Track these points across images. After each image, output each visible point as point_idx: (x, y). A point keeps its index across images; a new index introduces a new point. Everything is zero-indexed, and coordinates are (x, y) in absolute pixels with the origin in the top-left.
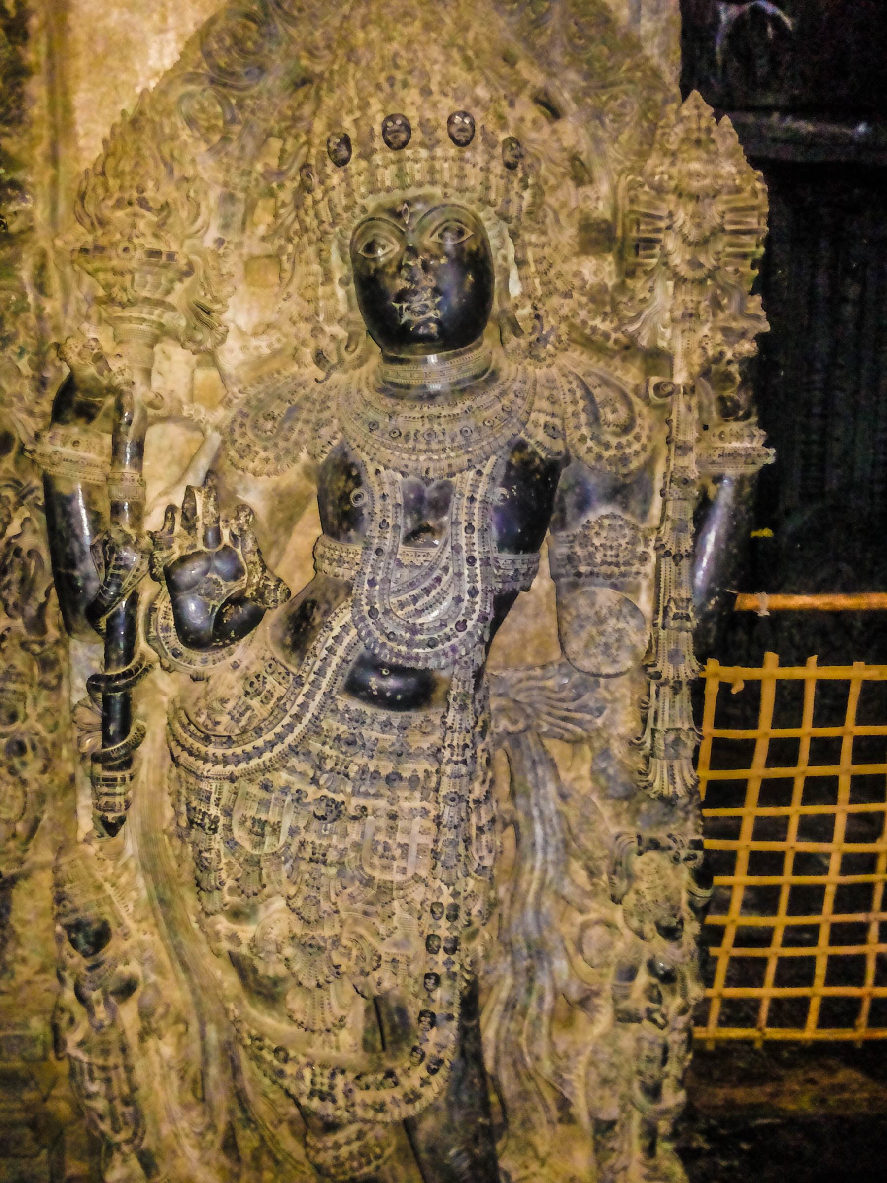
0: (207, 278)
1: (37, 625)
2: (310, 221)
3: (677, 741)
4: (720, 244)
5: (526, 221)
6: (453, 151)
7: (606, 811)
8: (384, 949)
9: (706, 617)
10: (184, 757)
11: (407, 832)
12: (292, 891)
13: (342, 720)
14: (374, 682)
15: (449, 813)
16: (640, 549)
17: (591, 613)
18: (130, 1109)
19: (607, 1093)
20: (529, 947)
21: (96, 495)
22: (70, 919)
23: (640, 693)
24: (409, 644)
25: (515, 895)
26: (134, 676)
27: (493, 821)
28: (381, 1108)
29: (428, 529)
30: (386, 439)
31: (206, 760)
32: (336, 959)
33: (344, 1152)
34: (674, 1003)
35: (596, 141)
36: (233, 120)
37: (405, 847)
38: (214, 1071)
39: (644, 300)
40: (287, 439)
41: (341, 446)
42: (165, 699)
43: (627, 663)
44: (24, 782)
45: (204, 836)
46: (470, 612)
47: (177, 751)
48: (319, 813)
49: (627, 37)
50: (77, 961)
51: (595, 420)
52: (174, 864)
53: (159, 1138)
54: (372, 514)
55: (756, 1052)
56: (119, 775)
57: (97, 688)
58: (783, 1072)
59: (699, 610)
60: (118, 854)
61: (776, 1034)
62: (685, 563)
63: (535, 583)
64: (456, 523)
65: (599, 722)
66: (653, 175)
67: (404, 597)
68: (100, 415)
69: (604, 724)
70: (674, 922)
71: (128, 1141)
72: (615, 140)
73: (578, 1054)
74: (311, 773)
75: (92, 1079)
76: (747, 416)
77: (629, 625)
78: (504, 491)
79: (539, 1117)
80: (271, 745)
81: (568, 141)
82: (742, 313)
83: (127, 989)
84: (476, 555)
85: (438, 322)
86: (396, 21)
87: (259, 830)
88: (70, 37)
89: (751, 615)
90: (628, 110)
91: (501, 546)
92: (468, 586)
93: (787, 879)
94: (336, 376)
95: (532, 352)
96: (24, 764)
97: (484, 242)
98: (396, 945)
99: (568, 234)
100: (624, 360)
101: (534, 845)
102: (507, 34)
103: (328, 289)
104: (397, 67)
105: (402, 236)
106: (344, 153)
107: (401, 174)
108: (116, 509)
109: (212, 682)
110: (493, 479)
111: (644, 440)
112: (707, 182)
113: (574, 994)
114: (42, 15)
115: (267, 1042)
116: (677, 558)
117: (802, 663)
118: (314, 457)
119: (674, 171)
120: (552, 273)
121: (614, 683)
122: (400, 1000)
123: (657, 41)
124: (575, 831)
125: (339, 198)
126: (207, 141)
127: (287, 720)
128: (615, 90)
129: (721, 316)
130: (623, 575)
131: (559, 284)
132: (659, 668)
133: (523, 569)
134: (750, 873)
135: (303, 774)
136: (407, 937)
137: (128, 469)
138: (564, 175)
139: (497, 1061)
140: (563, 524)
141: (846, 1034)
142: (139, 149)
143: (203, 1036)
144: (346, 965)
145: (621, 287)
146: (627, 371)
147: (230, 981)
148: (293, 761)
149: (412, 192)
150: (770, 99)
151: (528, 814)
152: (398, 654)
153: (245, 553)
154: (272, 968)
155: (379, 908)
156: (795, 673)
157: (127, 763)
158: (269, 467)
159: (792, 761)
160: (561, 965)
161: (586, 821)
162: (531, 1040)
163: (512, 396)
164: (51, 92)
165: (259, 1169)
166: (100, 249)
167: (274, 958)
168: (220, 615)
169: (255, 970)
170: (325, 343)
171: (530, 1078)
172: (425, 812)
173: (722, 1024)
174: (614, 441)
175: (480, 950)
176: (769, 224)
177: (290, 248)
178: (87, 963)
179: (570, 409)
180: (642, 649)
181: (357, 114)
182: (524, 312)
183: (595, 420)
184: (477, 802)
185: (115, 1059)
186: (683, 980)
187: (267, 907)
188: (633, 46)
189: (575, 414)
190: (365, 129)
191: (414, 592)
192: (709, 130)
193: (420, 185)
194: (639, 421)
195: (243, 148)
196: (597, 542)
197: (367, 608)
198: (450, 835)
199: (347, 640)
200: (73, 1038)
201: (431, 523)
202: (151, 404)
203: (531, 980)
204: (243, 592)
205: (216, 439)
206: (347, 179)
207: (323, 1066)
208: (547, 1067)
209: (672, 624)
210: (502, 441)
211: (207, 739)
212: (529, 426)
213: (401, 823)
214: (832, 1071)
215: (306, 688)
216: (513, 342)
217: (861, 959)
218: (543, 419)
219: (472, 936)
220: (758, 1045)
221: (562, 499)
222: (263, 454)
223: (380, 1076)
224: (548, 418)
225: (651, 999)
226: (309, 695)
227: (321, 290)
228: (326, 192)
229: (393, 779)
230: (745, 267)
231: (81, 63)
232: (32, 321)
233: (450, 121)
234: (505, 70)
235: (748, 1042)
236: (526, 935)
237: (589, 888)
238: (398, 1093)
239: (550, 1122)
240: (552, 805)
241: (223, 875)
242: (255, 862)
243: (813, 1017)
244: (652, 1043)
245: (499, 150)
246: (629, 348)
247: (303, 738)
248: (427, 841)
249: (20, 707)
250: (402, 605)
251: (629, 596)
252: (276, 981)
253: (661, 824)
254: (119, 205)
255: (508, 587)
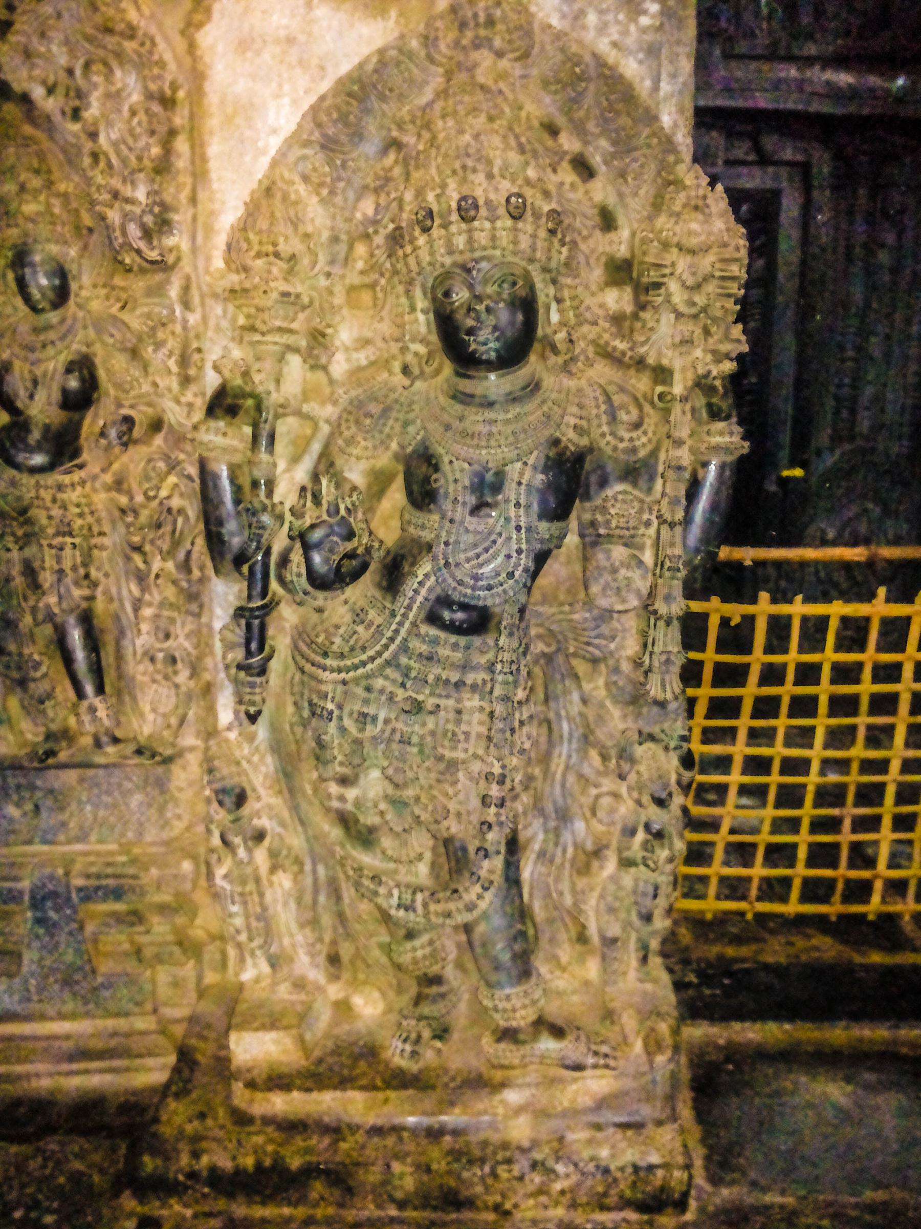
0: (322, 308)
1: (186, 567)
2: (399, 266)
3: (668, 661)
4: (711, 288)
5: (563, 270)
6: (509, 223)
7: (616, 712)
8: (452, 806)
9: (695, 569)
10: (308, 667)
11: (469, 723)
12: (386, 764)
13: (424, 641)
14: (447, 615)
15: (499, 709)
16: (646, 516)
17: (607, 564)
18: (262, 924)
19: (612, 918)
20: (556, 812)
21: (238, 472)
22: (217, 786)
23: (643, 625)
24: (474, 588)
25: (546, 772)
26: (268, 608)
27: (531, 717)
28: (448, 915)
29: (487, 505)
30: (458, 437)
31: (325, 669)
32: (417, 811)
33: (419, 954)
34: (663, 854)
35: (621, 195)
36: (339, 179)
37: (467, 734)
38: (322, 899)
39: (652, 329)
40: (381, 432)
41: (424, 441)
42: (287, 625)
43: (634, 602)
44: (177, 686)
45: (322, 723)
46: (517, 565)
47: (303, 662)
48: (407, 708)
49: (647, 110)
50: (221, 815)
51: (613, 418)
52: (293, 747)
53: (281, 945)
54: (446, 494)
55: (747, 922)
56: (258, 680)
57: (242, 616)
58: (767, 936)
59: (685, 564)
60: (251, 738)
61: (764, 907)
62: (678, 530)
63: (567, 540)
64: (507, 501)
65: (612, 646)
66: (661, 231)
67: (471, 554)
68: (241, 413)
69: (617, 649)
70: (664, 795)
71: (261, 947)
72: (636, 194)
73: (592, 889)
74: (400, 680)
75: (233, 903)
76: (727, 418)
77: (636, 575)
78: (542, 477)
79: (563, 936)
80: (372, 659)
81: (598, 197)
82: (727, 337)
83: (260, 836)
84: (522, 524)
85: (497, 351)
86: (467, 114)
87: (363, 719)
88: (206, 101)
89: (737, 566)
90: (645, 170)
91: (542, 516)
92: (515, 547)
93: (775, 779)
94: (419, 385)
95: (566, 368)
96: (176, 673)
97: (532, 288)
98: (460, 803)
99: (597, 274)
100: (638, 371)
101: (561, 737)
102: (552, 110)
103: (412, 316)
104: (468, 155)
105: (471, 287)
106: (429, 223)
107: (470, 240)
108: (255, 484)
109: (326, 614)
110: (535, 468)
111: (650, 434)
112: (703, 238)
113: (589, 846)
114: (186, 87)
115: (366, 872)
116: (672, 525)
117: (790, 601)
118: (402, 447)
119: (678, 229)
120: (582, 309)
121: (624, 617)
122: (462, 840)
123: (674, 101)
124: (592, 726)
125: (426, 258)
126: (318, 194)
127: (384, 641)
128: (636, 154)
129: (711, 340)
130: (633, 536)
131: (588, 315)
132: (656, 607)
133: (556, 533)
134: (744, 772)
135: (394, 681)
136: (467, 797)
137: (264, 456)
138: (594, 227)
139: (531, 895)
140: (587, 497)
141: (822, 909)
142: (272, 214)
143: (314, 872)
144: (424, 816)
145: (635, 316)
146: (639, 380)
147: (335, 833)
148: (388, 671)
149: (477, 254)
150: (811, 49)
151: (558, 715)
152: (465, 595)
153: (356, 522)
154: (370, 819)
155: (448, 777)
156: (783, 609)
157: (262, 671)
158: (367, 453)
159: (781, 681)
160: (580, 826)
161: (600, 719)
162: (558, 879)
163: (550, 404)
164: (192, 147)
165: (355, 971)
166: (245, 291)
167: (372, 811)
168: (339, 566)
169: (357, 821)
170: (409, 358)
171: (556, 908)
172: (482, 709)
173: (718, 898)
174: (627, 435)
175: (520, 809)
176: (748, 272)
177: (383, 281)
178: (231, 817)
179: (594, 412)
180: (645, 592)
181: (438, 191)
182: (561, 336)
183: (613, 418)
184: (519, 703)
185: (250, 887)
186: (670, 838)
187: (366, 776)
188: (652, 118)
189: (598, 416)
190: (444, 206)
191: (478, 551)
192: (705, 197)
193: (485, 248)
194: (646, 420)
195: (346, 200)
196: (613, 511)
197: (442, 562)
198: (500, 725)
199: (428, 584)
200: (220, 872)
201: (489, 500)
202: (282, 406)
203: (558, 836)
204: (355, 549)
205: (325, 429)
206: (431, 242)
207: (408, 886)
208: (568, 900)
209: (667, 574)
210: (542, 440)
211: (325, 655)
212: (563, 427)
213: (465, 717)
214: (808, 937)
215: (398, 619)
216: (553, 360)
217: (836, 846)
218: (573, 421)
219: (516, 797)
220: (749, 916)
221: (587, 478)
222: (363, 443)
223: (448, 893)
224: (577, 421)
225: (646, 850)
226: (401, 624)
227: (407, 317)
228: (414, 250)
229: (459, 685)
230: (730, 304)
231: (213, 122)
232: (178, 328)
233: (508, 200)
234: (550, 143)
235: (742, 914)
236: (555, 803)
237: (601, 768)
238: (460, 905)
239: (570, 940)
240: (575, 706)
241: (336, 752)
242: (358, 742)
243: (795, 893)
244: (646, 882)
245: (544, 220)
246: (640, 363)
247: (395, 656)
248: (483, 730)
249: (172, 629)
250: (468, 560)
251: (636, 552)
252: (372, 830)
253: (656, 723)
254: (258, 255)
255: (545, 547)
